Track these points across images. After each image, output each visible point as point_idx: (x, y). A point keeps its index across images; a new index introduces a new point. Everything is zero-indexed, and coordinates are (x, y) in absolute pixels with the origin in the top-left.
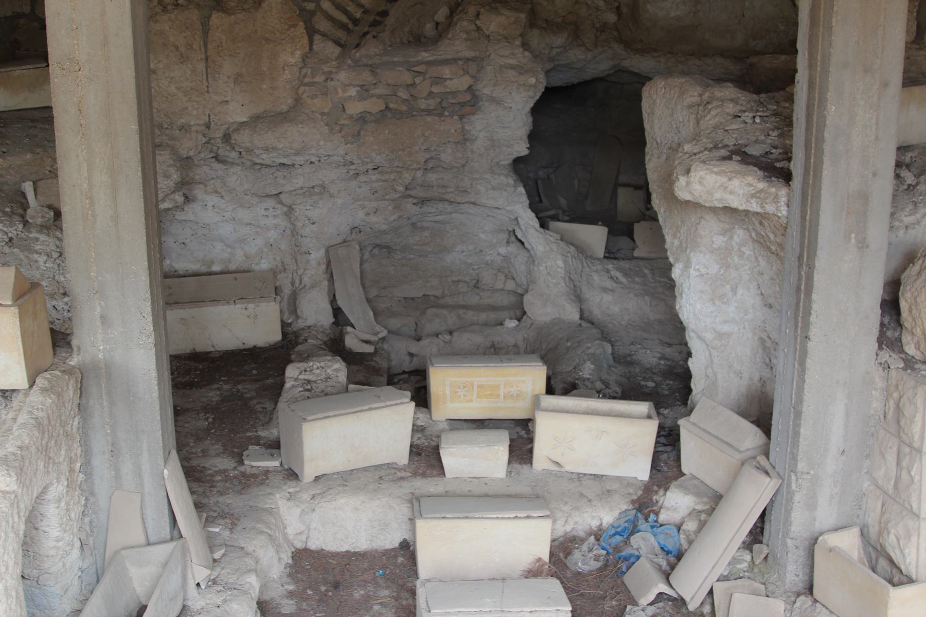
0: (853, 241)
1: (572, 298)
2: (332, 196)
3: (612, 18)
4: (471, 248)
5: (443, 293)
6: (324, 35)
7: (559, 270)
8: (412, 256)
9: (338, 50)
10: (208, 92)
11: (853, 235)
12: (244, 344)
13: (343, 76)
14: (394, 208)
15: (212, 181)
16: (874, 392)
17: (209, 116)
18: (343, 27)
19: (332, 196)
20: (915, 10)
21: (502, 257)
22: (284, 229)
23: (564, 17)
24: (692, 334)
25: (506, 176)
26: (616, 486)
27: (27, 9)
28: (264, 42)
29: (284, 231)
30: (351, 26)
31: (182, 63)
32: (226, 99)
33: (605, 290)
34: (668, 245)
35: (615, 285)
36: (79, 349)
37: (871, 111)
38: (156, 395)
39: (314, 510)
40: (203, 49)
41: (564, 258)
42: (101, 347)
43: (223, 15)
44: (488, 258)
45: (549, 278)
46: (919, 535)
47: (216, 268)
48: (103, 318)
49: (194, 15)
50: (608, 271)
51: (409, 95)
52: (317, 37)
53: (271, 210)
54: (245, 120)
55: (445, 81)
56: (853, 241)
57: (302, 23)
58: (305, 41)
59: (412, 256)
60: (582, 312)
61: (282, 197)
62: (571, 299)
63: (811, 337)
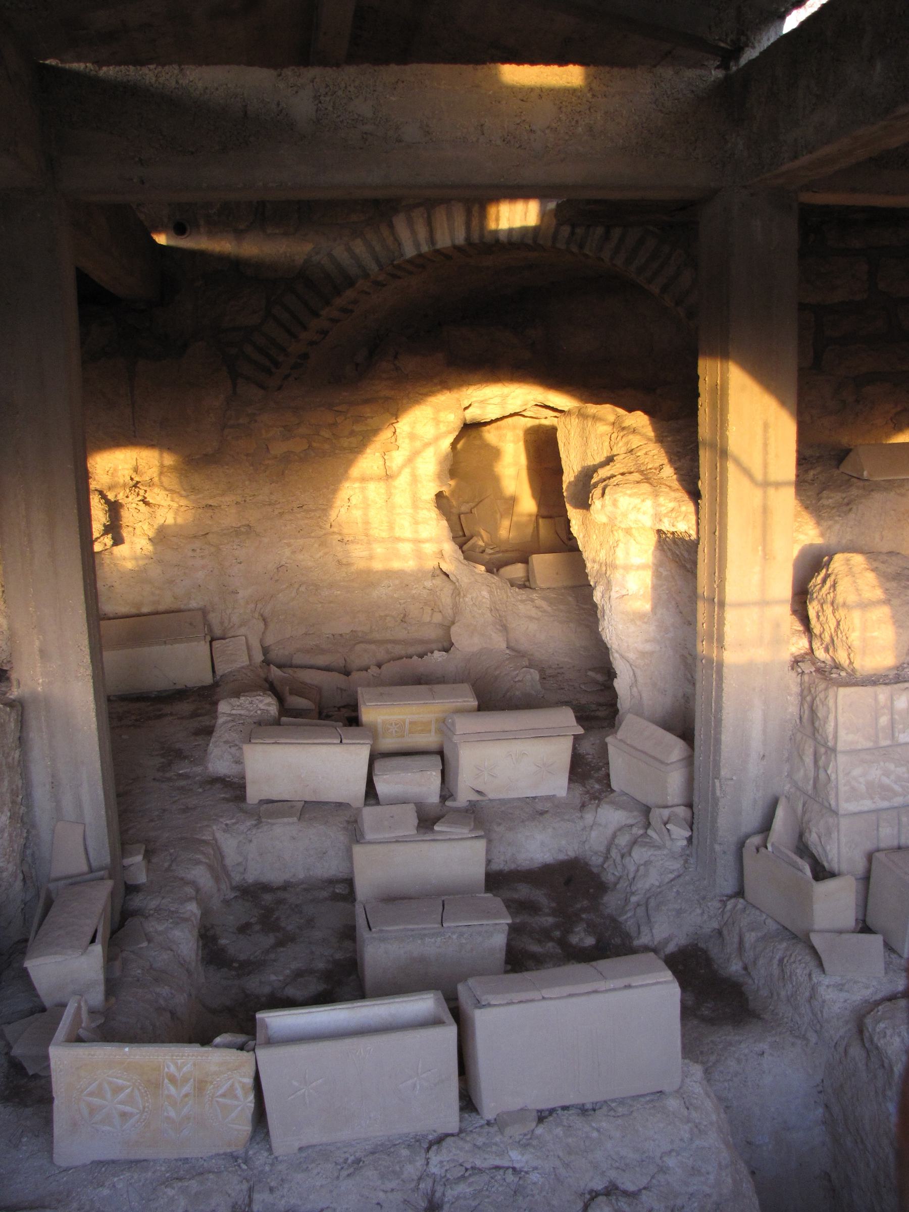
1: (498, 627)
2: (258, 535)
4: (397, 582)
5: (371, 627)
7: (484, 600)
8: (339, 592)
12: (175, 684)
14: (320, 545)
16: (789, 698)
19: (258, 535)
21: (428, 591)
22: (212, 569)
24: (616, 655)
25: (429, 510)
26: (548, 805)
29: (212, 571)
33: (531, 618)
34: (589, 570)
35: (540, 614)
36: (19, 683)
38: (94, 726)
39: (251, 841)
41: (489, 588)
42: (41, 681)
44: (414, 592)
45: (475, 609)
46: (838, 831)
47: (145, 610)
48: (42, 652)
50: (532, 601)
51: (331, 434)
53: (198, 550)
55: (366, 420)
59: (339, 592)
60: (508, 641)
61: (210, 536)
62: (497, 629)
63: (726, 647)
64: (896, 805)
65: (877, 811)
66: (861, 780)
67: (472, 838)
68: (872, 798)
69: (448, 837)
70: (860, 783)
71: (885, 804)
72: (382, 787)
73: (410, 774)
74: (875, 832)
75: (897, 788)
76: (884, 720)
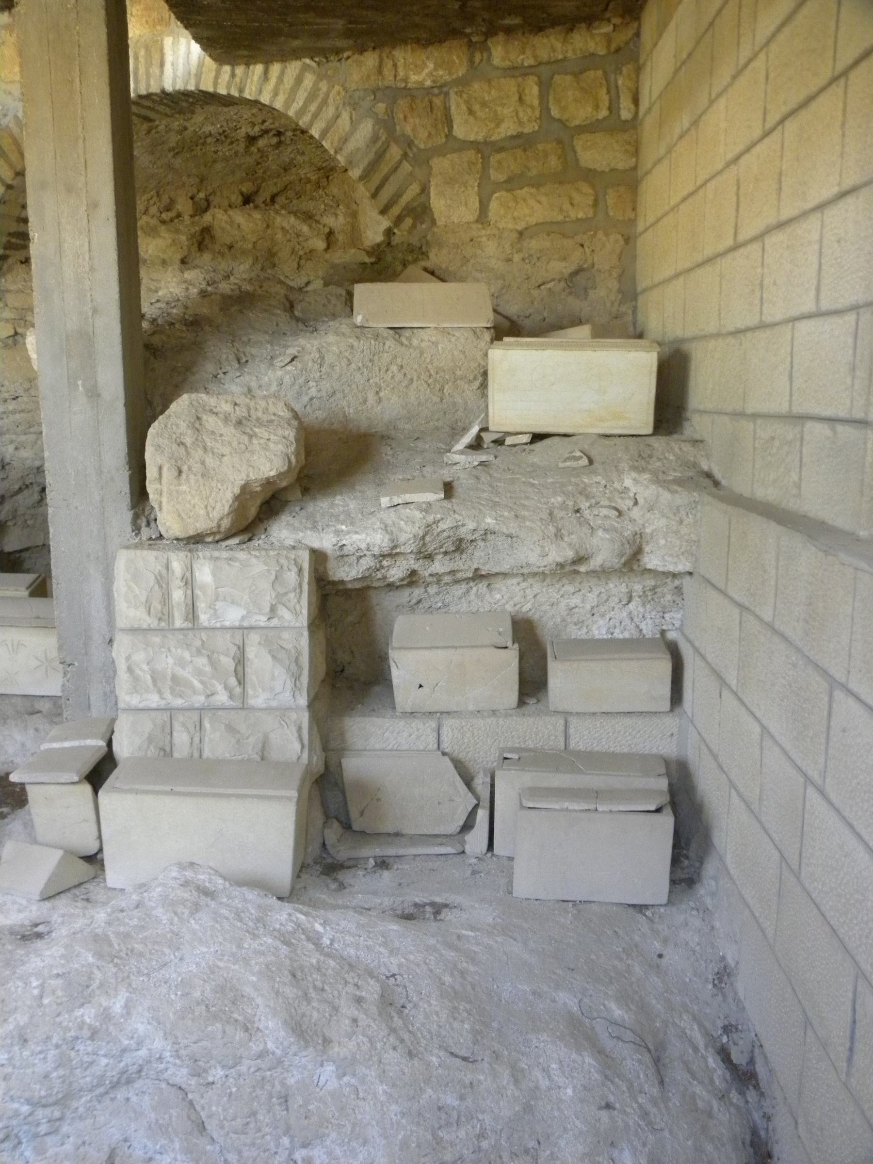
0: (81, 389)
11: (80, 383)
20: (476, 184)
23: (254, 243)
56: (81, 389)
64: (197, 705)
65: (170, 710)
68: (160, 692)
70: (144, 671)
71: (179, 702)
74: (169, 737)
75: (196, 684)
76: (178, 595)
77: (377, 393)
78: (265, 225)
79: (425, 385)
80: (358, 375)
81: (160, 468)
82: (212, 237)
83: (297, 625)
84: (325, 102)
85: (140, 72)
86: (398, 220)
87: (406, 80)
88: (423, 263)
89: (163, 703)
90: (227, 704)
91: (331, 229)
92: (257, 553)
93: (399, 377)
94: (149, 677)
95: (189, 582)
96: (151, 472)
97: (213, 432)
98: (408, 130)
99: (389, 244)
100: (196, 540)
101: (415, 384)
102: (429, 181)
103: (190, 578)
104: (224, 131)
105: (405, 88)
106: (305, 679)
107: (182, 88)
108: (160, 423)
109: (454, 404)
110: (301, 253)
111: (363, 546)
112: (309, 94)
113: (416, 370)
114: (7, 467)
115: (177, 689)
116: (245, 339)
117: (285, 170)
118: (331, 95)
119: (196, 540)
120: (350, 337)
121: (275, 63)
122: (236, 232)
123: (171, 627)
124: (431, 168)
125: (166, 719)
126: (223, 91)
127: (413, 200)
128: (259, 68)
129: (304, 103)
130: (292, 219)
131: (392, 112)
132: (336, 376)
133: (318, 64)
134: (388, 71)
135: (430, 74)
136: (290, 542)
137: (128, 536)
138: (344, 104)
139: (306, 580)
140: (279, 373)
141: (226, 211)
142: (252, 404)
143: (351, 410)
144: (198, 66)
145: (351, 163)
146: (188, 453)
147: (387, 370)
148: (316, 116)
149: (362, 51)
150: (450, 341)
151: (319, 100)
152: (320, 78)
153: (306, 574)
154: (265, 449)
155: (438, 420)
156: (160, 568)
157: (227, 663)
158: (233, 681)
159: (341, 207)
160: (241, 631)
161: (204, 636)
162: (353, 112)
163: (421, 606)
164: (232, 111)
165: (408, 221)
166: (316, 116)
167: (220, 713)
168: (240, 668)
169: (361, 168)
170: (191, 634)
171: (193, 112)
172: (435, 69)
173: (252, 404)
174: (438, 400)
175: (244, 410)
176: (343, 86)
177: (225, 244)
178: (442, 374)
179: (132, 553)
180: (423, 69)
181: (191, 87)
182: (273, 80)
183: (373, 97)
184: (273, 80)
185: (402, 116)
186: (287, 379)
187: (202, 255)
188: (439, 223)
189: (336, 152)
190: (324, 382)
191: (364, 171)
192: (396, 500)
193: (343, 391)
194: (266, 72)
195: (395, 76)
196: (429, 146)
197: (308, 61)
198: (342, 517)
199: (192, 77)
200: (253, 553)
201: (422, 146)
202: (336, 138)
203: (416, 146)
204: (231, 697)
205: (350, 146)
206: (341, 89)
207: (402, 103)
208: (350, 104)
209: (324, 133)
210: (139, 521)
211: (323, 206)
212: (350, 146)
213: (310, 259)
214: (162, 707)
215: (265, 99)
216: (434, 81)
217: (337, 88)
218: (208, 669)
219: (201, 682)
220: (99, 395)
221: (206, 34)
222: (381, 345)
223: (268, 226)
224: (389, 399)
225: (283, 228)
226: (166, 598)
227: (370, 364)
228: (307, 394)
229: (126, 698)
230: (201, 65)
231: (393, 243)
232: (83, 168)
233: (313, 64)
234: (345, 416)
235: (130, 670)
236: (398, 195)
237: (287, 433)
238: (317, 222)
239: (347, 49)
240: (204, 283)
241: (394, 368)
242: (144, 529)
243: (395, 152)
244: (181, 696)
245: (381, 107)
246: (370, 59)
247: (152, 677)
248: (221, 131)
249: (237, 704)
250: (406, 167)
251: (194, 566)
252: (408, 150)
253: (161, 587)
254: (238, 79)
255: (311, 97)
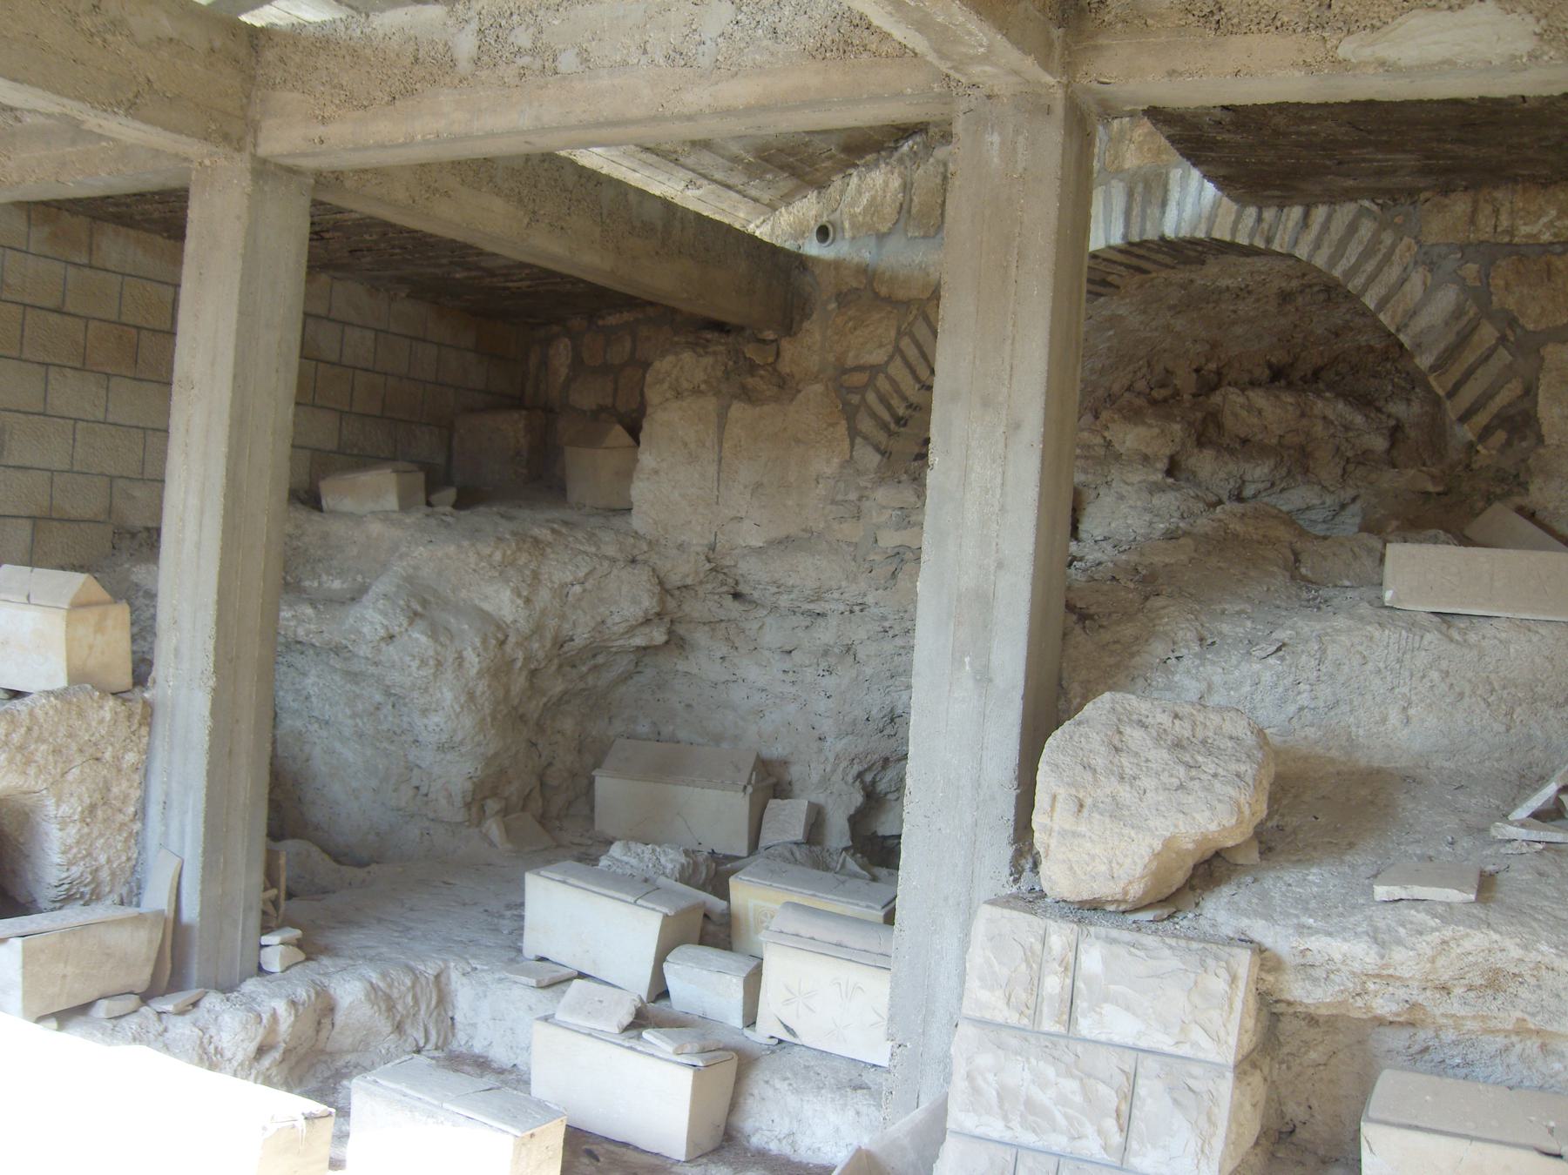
0: (967, 668)
3: (1379, 443)
6: (865, 438)
9: (877, 457)
10: (717, 503)
11: (967, 659)
13: (882, 495)
15: (723, 624)
17: (716, 535)
18: (884, 426)
23: (1280, 436)
27: (609, 401)
28: (793, 443)
30: (892, 426)
31: (690, 464)
32: (739, 515)
37: (994, 466)
40: (716, 448)
43: (746, 407)
49: (710, 404)
52: (859, 440)
54: (761, 545)
56: (967, 668)
57: (844, 422)
58: (847, 442)
64: (1055, 1149)
65: (1017, 1147)
66: (990, 1077)
67: (678, 1063)
68: (1005, 1118)
69: (651, 1051)
71: (1029, 1138)
72: (673, 983)
73: (705, 972)
76: (1053, 984)
77: (1404, 709)
78: (1298, 413)
79: (1483, 705)
80: (1377, 681)
81: (1054, 798)
82: (1220, 426)
83: (1219, 1059)
84: (1387, 259)
85: (1134, 213)
86: (1485, 434)
87: (1511, 232)
88: (1517, 500)
89: (1007, 1136)
90: (1098, 1156)
91: (1398, 420)
92: (1173, 942)
93: (1444, 687)
94: (994, 1093)
95: (1071, 968)
96: (1041, 798)
97: (1137, 754)
98: (1511, 303)
99: (1468, 467)
100: (1089, 909)
101: (1467, 700)
102: (1538, 379)
103: (1072, 960)
104: (1247, 286)
105: (1509, 244)
106: (1218, 1144)
107: (1188, 235)
108: (1064, 732)
109: (1529, 737)
110: (1350, 454)
111: (1337, 957)
112: (1366, 247)
113: (1470, 681)
114: (897, 720)
115: (1031, 1118)
116: (1218, 608)
117: (1337, 335)
118: (1397, 251)
119: (1089, 909)
120: (1370, 623)
121: (1320, 205)
122: (1256, 421)
123: (1036, 1029)
124: (1542, 359)
125: (1008, 1158)
126: (1243, 240)
127: (1510, 405)
128: (1296, 212)
129: (1357, 260)
130: (1341, 406)
131: (1488, 276)
132: (1342, 679)
133: (1382, 206)
134: (1485, 221)
135: (1551, 224)
136: (1227, 931)
137: (1004, 880)
138: (1416, 263)
139: (1241, 994)
140: (1256, 667)
141: (1243, 390)
142: (1200, 718)
143: (1361, 732)
144: (1212, 208)
145: (1419, 345)
146: (1096, 780)
147: (1424, 677)
148: (1372, 279)
149: (1446, 191)
150: (1530, 641)
151: (1380, 256)
152: (1383, 227)
153: (1242, 984)
154: (1208, 790)
155: (1498, 760)
156: (1033, 940)
157: (1109, 1096)
158: (1110, 1124)
159: (1417, 390)
160: (1134, 1054)
161: (1079, 1049)
162: (1429, 275)
163: (1427, 1057)
164: (1259, 263)
165: (1500, 436)
166: (1372, 279)
167: (1086, 1166)
168: (1124, 1108)
169: (1435, 353)
170: (1063, 1042)
171: (1203, 263)
172: (1558, 218)
173: (1200, 718)
174: (1502, 729)
175: (1187, 725)
176: (1415, 238)
177: (1237, 436)
178: (1513, 690)
179: (997, 911)
180: (1540, 217)
181: (1200, 234)
182: (1315, 228)
183: (1459, 255)
184: (1315, 228)
185: (1502, 283)
186: (1267, 677)
187: (1201, 451)
188: (1548, 441)
189: (1398, 330)
190: (1323, 686)
191: (1437, 359)
192: (1398, 892)
193: (1351, 701)
194: (1306, 216)
195: (1496, 227)
196: (1542, 326)
197: (1366, 203)
198: (1313, 904)
199: (1203, 220)
200: (1168, 940)
201: (1531, 327)
202: (1400, 310)
203: (1522, 327)
204: (1105, 1148)
205: (1421, 322)
206: (1413, 241)
207: (1504, 263)
208: (1424, 263)
209: (1383, 303)
210: (1023, 861)
211: (1390, 388)
212: (1421, 322)
213: (1363, 464)
214: (1006, 1139)
215: (1302, 252)
216: (1555, 235)
217: (1406, 240)
218: (1078, 1099)
219: (1066, 1116)
220: (990, 680)
221: (1222, 172)
222: (1417, 638)
223: (1303, 415)
224: (1423, 721)
225: (1325, 418)
226: (1036, 984)
227: (1398, 666)
228: (1295, 701)
229: (959, 1118)
230: (1216, 205)
231: (1475, 466)
232: (1006, 377)
233: (1375, 208)
234: (1349, 739)
235: (969, 1077)
236: (1488, 396)
237: (1242, 768)
238: (1379, 410)
239: (1425, 189)
240: (1177, 514)
241: (1435, 675)
242: (1027, 874)
243: (1488, 333)
244: (1034, 1131)
245: (1471, 269)
246: (1460, 205)
247: (998, 1093)
248: (1243, 286)
249: (1113, 1160)
250: (1504, 356)
251: (1081, 946)
252: (1509, 332)
253: (1030, 966)
254: (1265, 226)
255: (1366, 254)
